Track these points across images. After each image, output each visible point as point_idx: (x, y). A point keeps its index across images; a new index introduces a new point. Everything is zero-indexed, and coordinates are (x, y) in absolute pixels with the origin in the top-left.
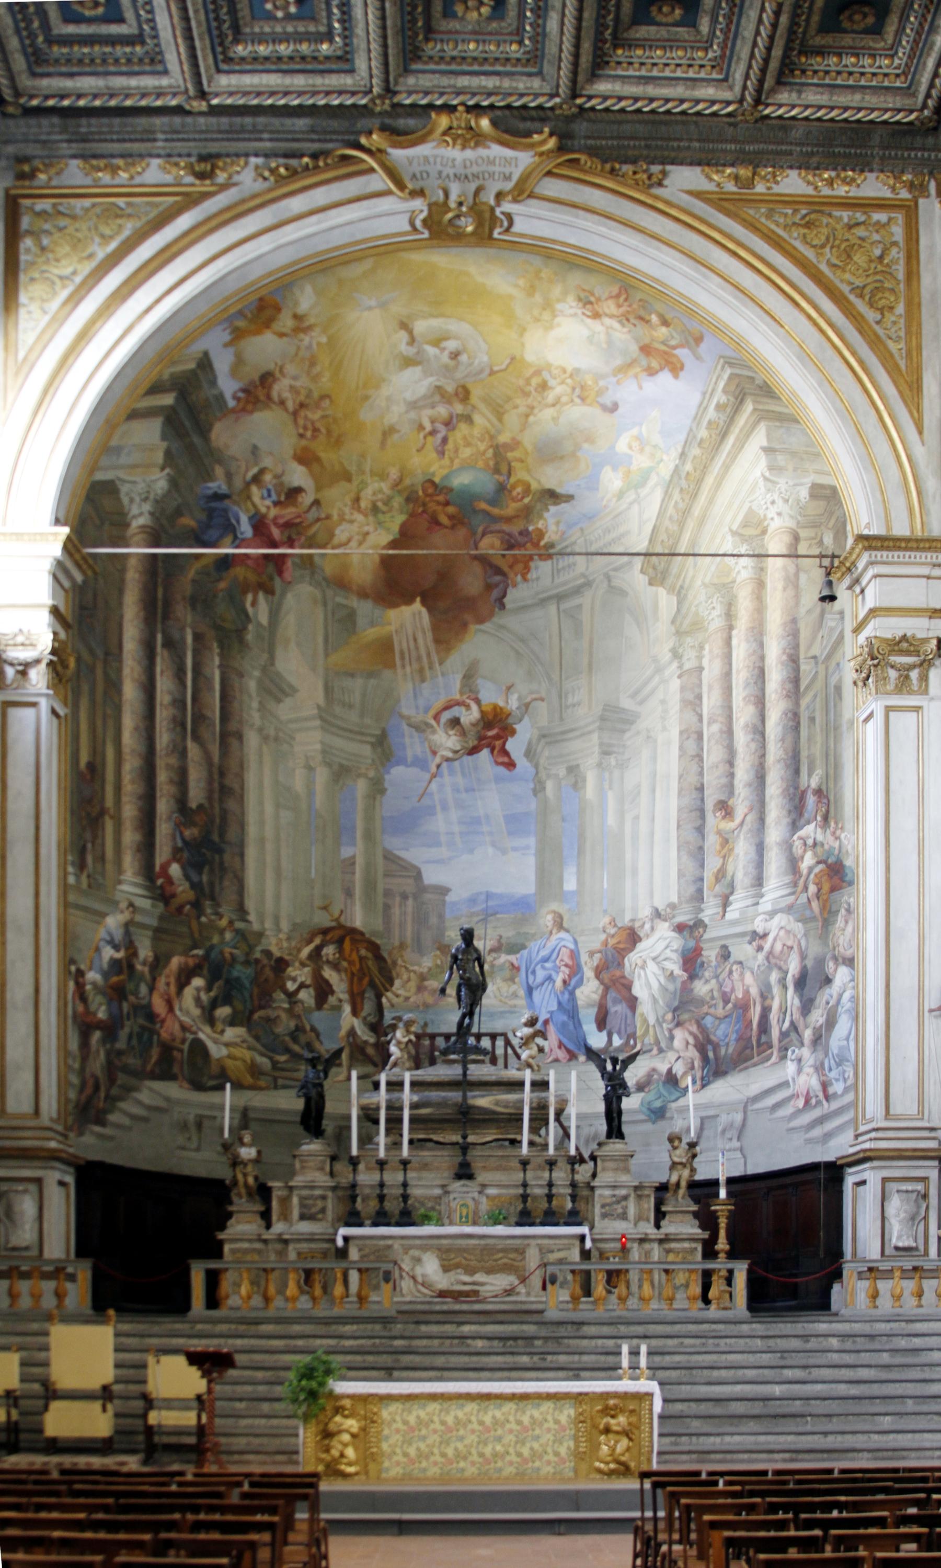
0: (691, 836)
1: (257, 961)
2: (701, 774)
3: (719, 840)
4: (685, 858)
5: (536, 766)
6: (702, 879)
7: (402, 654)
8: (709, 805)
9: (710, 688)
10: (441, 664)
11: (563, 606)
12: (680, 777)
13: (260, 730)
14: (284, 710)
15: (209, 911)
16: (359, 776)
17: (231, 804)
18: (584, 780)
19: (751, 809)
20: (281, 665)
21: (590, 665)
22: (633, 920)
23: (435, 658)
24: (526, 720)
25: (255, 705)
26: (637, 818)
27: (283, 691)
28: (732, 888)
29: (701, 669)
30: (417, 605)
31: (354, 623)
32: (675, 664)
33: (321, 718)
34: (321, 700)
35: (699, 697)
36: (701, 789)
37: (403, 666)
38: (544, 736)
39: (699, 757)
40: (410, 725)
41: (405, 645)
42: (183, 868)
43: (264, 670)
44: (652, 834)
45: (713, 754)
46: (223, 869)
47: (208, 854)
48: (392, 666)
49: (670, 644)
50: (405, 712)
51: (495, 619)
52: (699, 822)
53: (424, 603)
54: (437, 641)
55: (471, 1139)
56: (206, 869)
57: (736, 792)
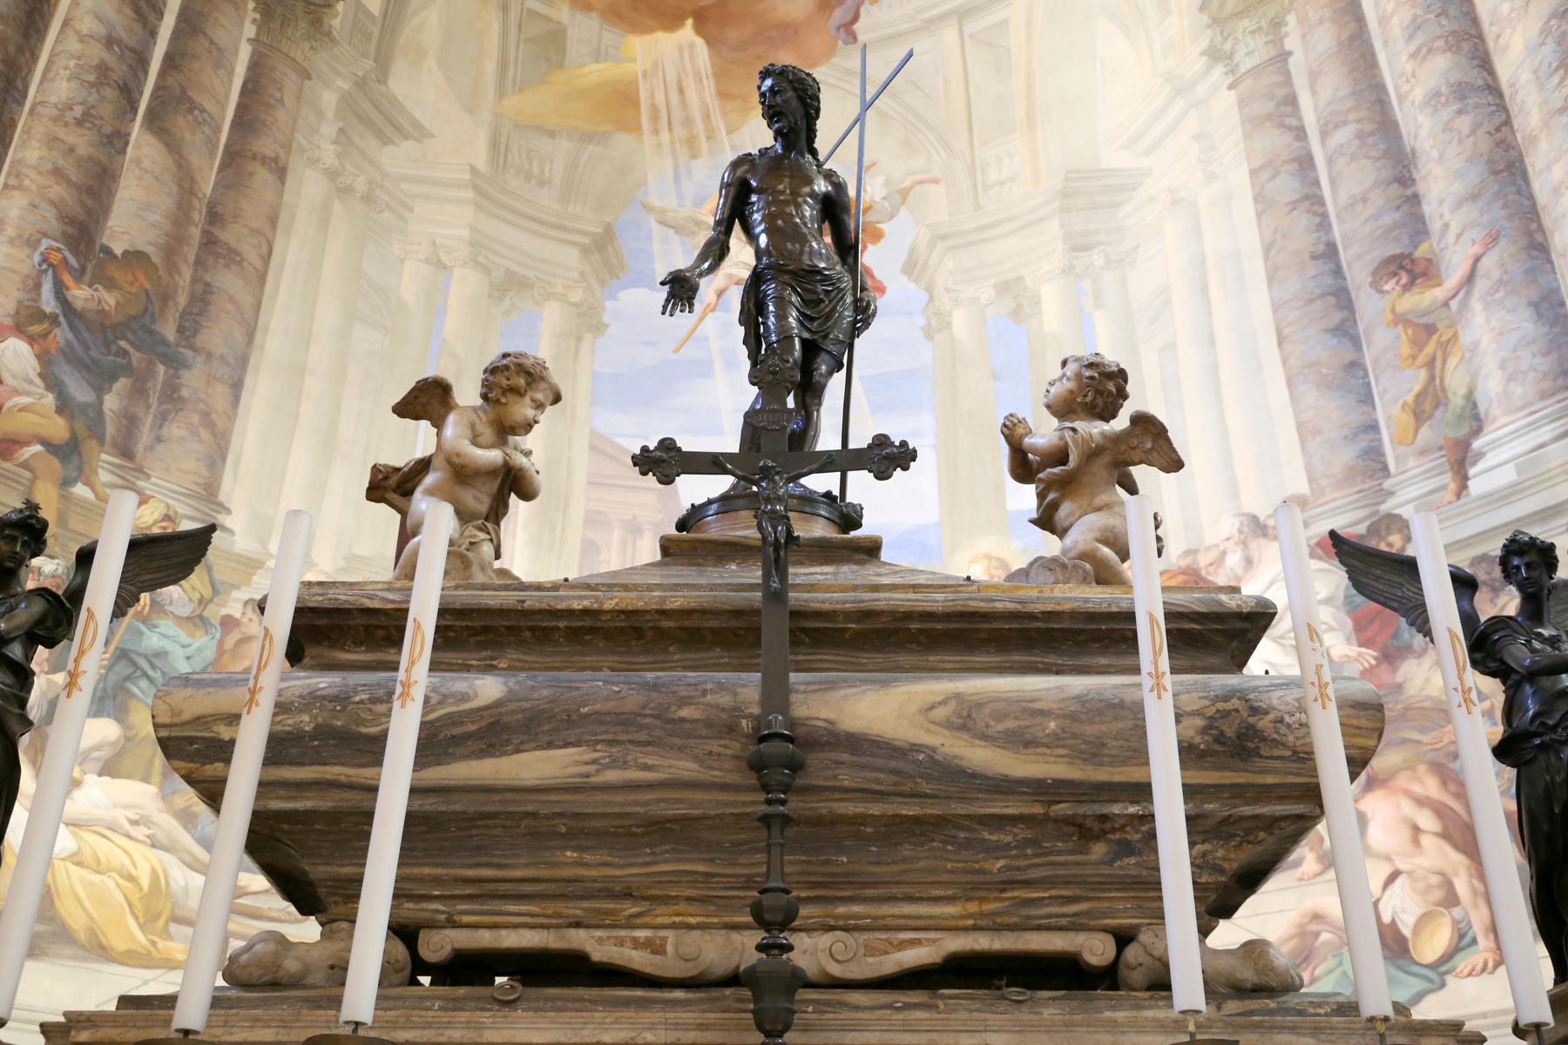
0: (1324, 351)
1: (228, 623)
2: (1324, 224)
3: (1403, 335)
4: (1311, 396)
5: (929, 289)
6: (1373, 427)
7: (654, 109)
8: (1358, 274)
9: (1313, 77)
10: (730, 132)
11: (969, 28)
12: (1267, 249)
13: (332, 174)
14: (396, 158)
15: (104, 476)
16: (548, 297)
17: (227, 281)
18: (1037, 302)
19: (1493, 239)
20: (401, 84)
21: (1031, 119)
22: (1189, 553)
23: (719, 122)
24: (903, 213)
25: (329, 129)
26: (1171, 346)
27: (398, 129)
28: (1475, 420)
29: (1284, 56)
30: (687, 32)
31: (563, 51)
32: (1220, 69)
33: (476, 188)
34: (482, 164)
35: (1292, 101)
36: (1331, 251)
37: (656, 132)
38: (942, 238)
39: (1313, 200)
40: (662, 223)
41: (660, 98)
42: (44, 358)
43: (361, 84)
44: (1214, 370)
45: (1349, 182)
46: (171, 394)
47: (136, 357)
48: (634, 127)
49: (1204, 43)
50: (655, 201)
51: (835, 60)
52: (1337, 317)
53: (699, 29)
54: (723, 95)
55: (811, 951)
56: (121, 384)
57: (1435, 226)
